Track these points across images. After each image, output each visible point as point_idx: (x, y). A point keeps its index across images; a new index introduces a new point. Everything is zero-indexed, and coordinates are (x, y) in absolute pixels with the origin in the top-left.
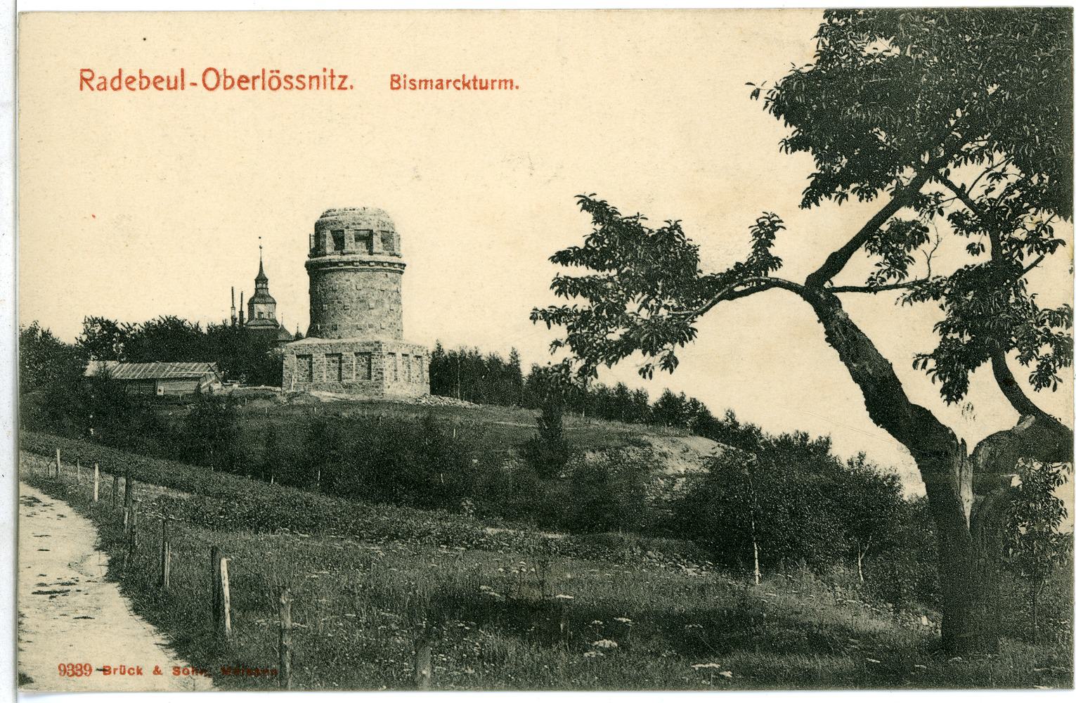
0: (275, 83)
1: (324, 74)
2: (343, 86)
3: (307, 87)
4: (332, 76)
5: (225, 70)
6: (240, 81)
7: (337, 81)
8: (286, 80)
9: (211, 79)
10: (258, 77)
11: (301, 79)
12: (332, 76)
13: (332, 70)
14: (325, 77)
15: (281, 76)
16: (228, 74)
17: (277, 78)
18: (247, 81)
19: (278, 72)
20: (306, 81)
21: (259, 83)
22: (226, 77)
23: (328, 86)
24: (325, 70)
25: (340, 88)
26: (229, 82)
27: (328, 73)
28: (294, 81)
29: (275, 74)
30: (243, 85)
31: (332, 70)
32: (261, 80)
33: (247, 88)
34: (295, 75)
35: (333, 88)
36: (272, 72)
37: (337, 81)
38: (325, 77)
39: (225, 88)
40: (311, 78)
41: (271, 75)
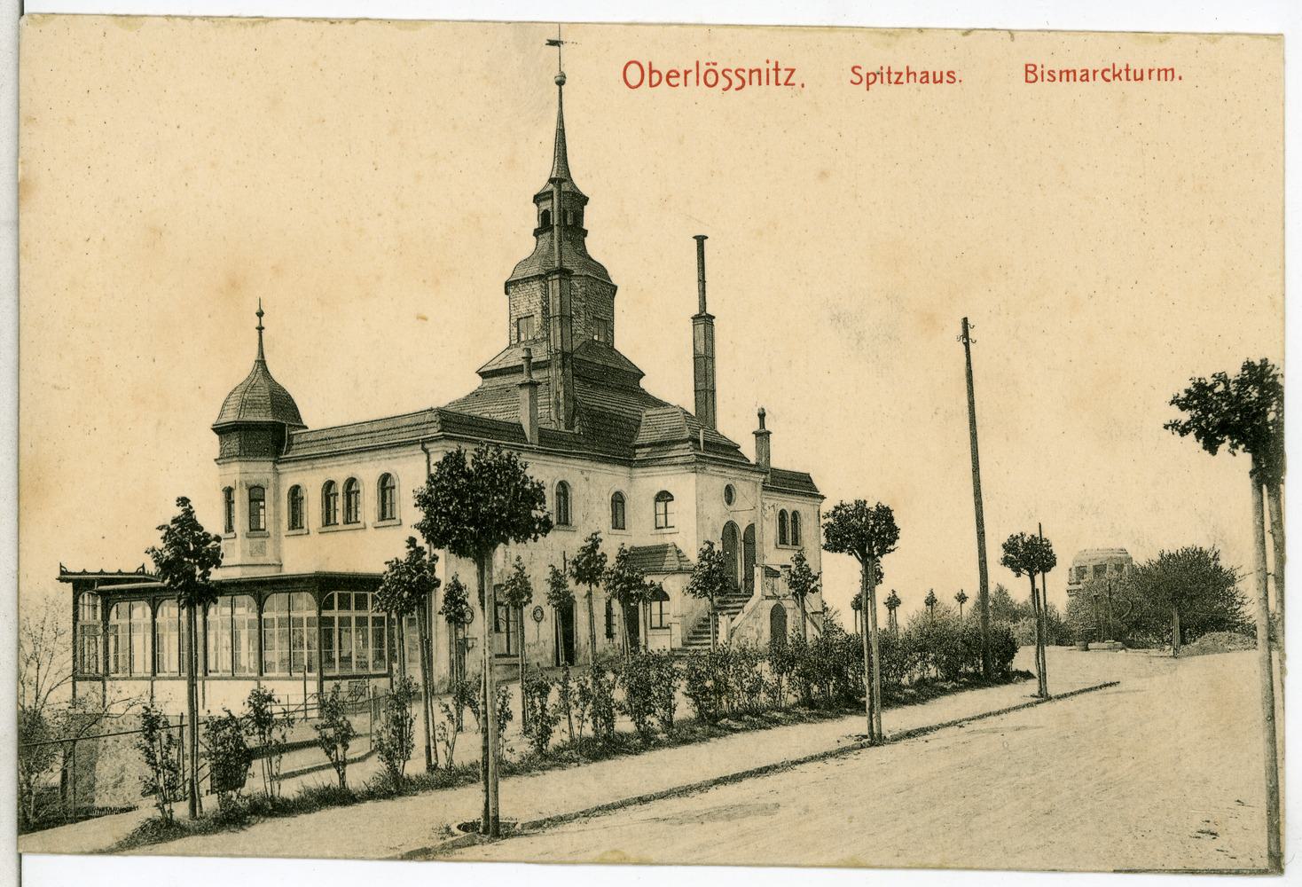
0: (711, 78)
1: (767, 66)
2: (790, 82)
3: (747, 80)
4: (777, 70)
5: (650, 64)
6: (668, 76)
7: (783, 76)
8: (724, 76)
9: (634, 75)
10: (690, 71)
11: (740, 73)
12: (777, 70)
13: (777, 63)
14: (768, 70)
15: (719, 69)
16: (653, 69)
17: (714, 71)
18: (678, 76)
19: (715, 64)
20: (746, 76)
21: (692, 77)
22: (651, 72)
23: (772, 78)
24: (768, 62)
25: (786, 84)
26: (656, 78)
27: (772, 66)
28: (732, 75)
29: (711, 67)
30: (673, 81)
31: (777, 63)
32: (695, 72)
33: (678, 85)
34: (734, 69)
35: (777, 84)
36: (708, 64)
37: (783, 76)
38: (768, 70)
39: (651, 86)
40: (751, 72)
41: (709, 67)
